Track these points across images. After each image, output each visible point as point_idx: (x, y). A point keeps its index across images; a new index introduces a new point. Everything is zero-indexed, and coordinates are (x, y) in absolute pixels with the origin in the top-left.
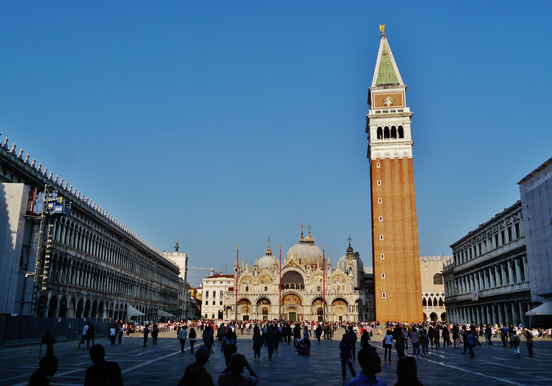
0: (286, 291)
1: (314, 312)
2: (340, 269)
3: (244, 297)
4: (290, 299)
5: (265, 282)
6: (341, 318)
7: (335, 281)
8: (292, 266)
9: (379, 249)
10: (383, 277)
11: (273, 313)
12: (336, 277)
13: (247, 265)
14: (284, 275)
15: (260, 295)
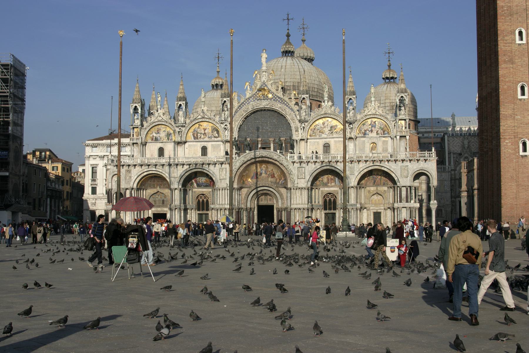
0: (249, 155)
1: (317, 202)
2: (377, 103)
3: (153, 170)
4: (261, 174)
5: (202, 136)
6: (377, 216)
7: (366, 131)
8: (266, 98)
9: (511, 15)
10: (523, 94)
11: (221, 206)
12: (369, 121)
13: (159, 99)
14: (245, 118)
15: (190, 165)
